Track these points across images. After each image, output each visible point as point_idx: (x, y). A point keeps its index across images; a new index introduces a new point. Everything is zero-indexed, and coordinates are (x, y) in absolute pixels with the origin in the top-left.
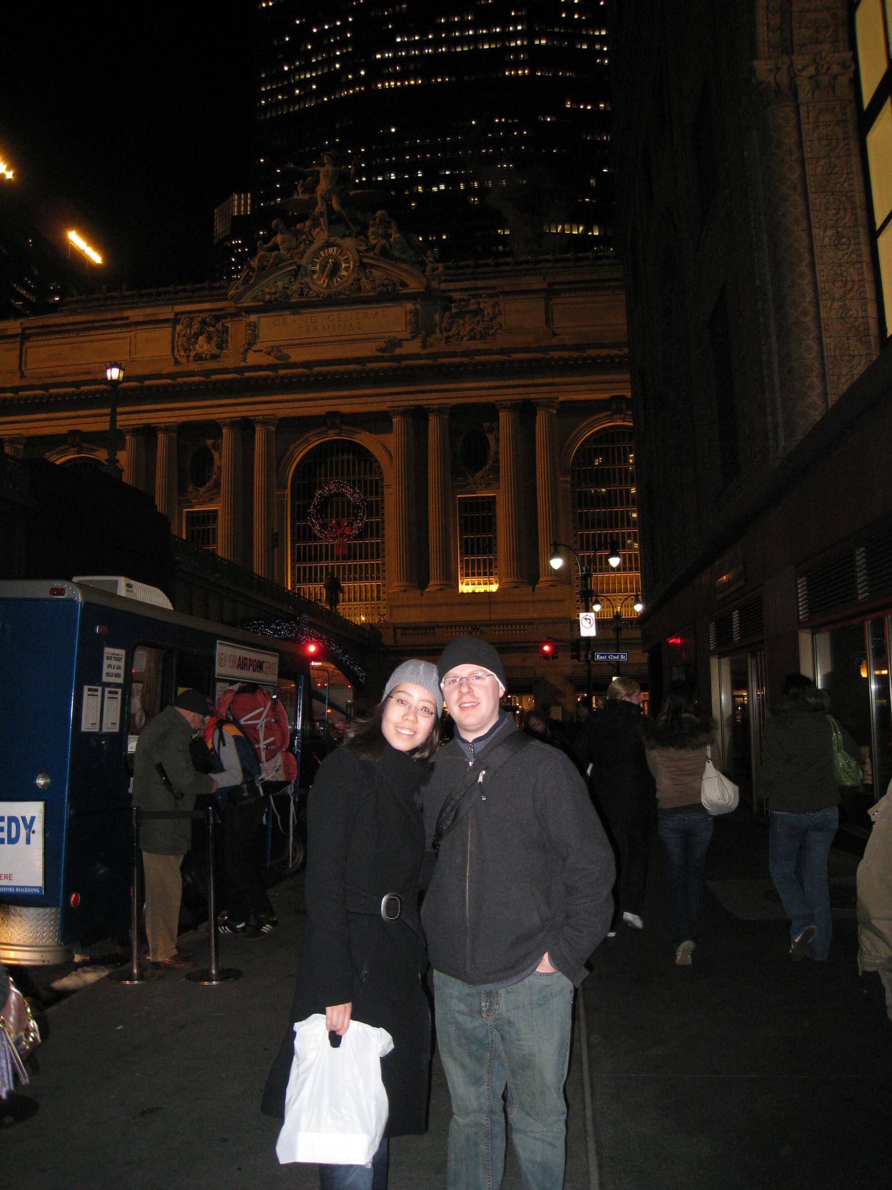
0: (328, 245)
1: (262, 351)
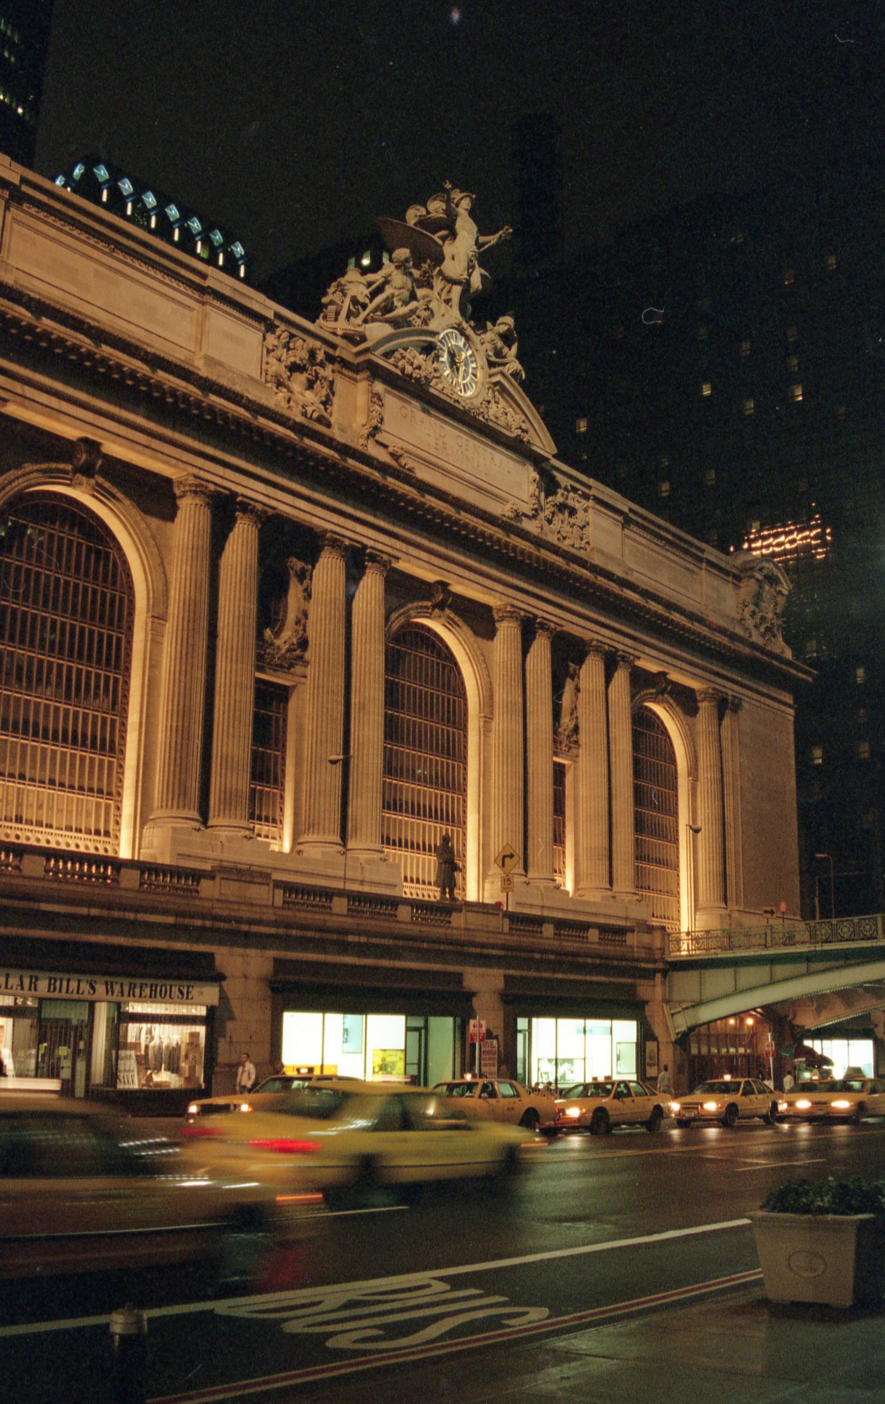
1: (386, 447)
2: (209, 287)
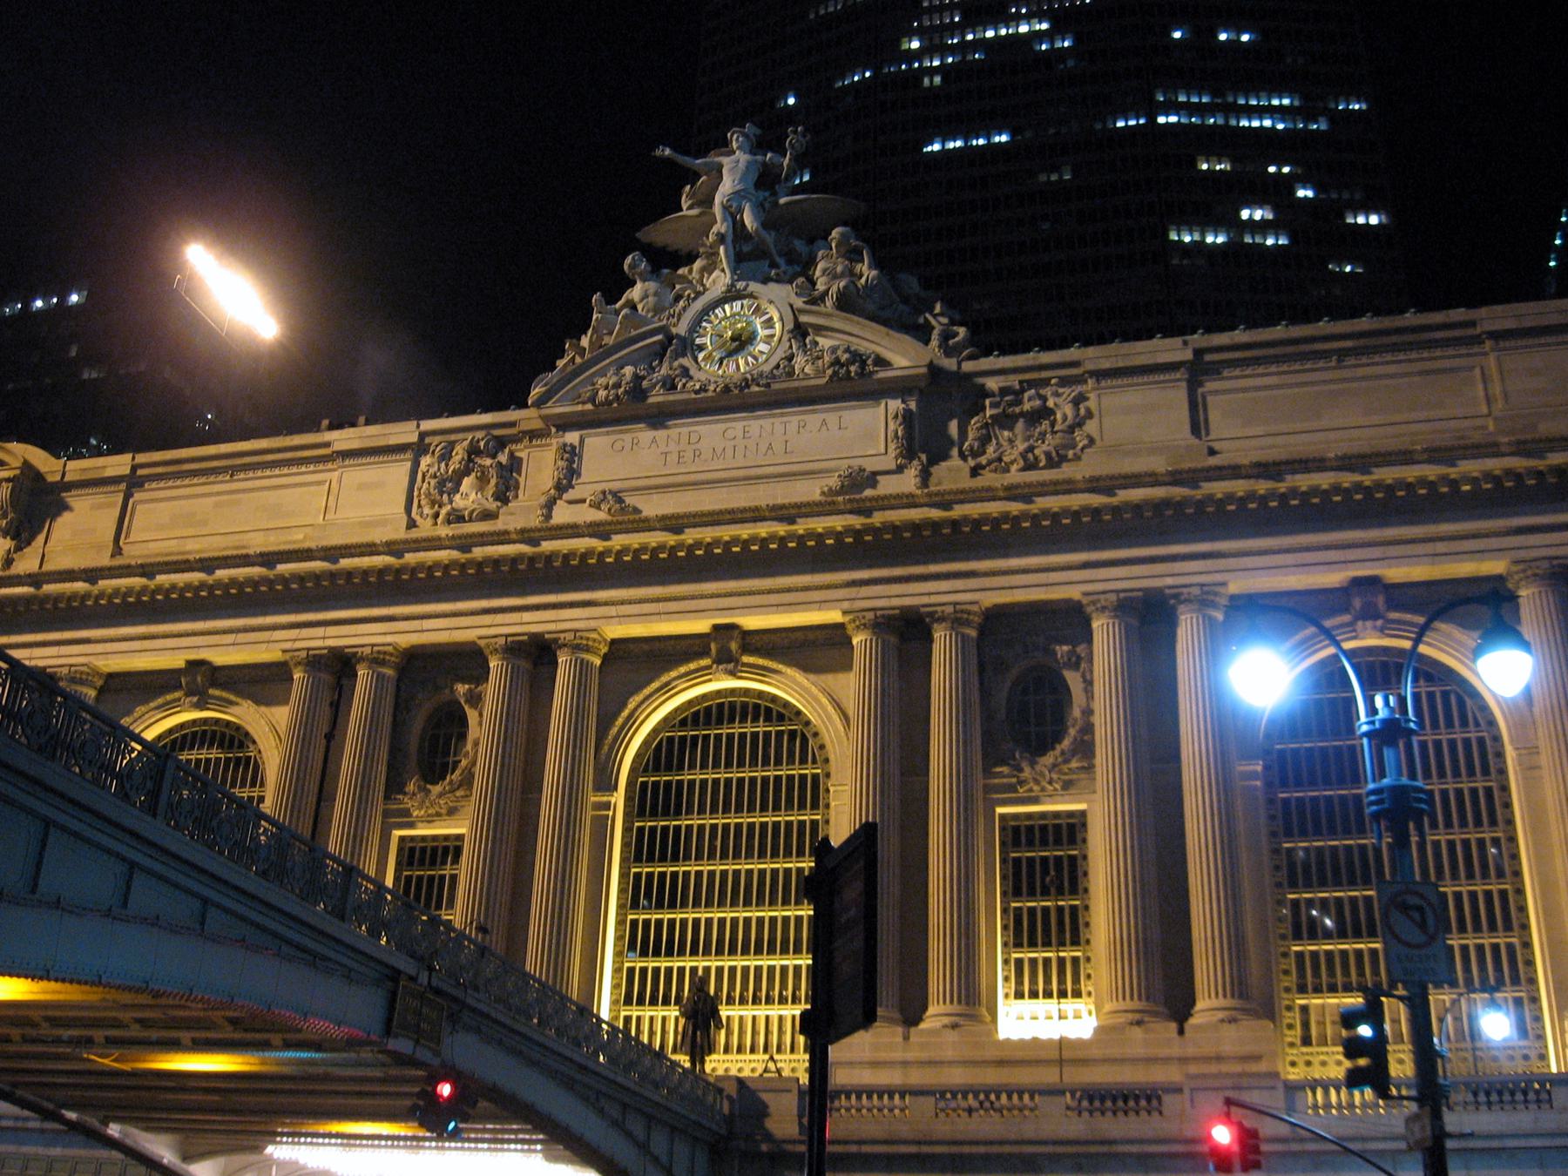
0: (731, 295)
1: (584, 501)
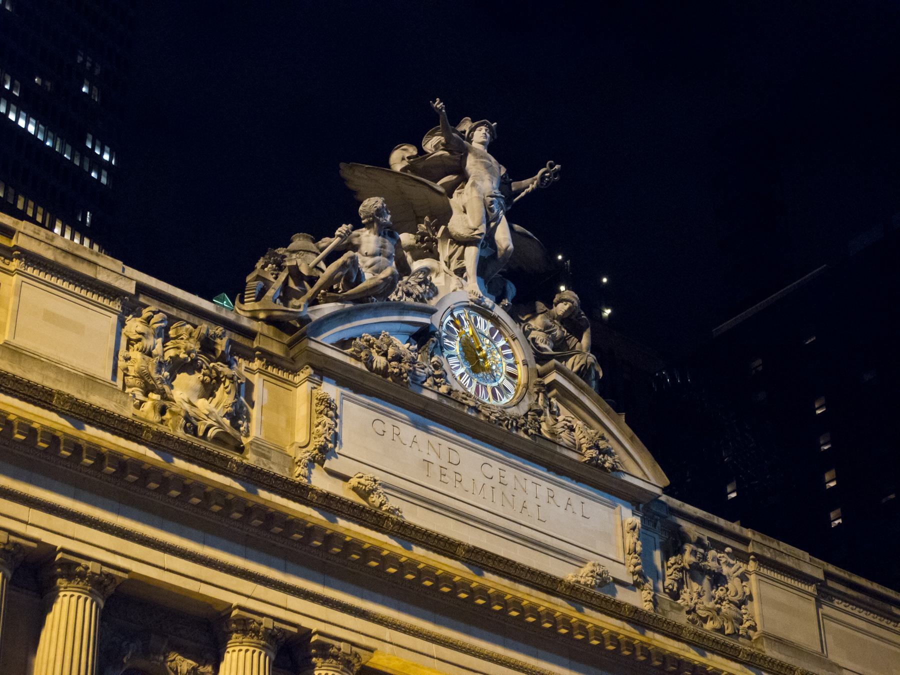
1: (346, 479)
2: (16, 248)
